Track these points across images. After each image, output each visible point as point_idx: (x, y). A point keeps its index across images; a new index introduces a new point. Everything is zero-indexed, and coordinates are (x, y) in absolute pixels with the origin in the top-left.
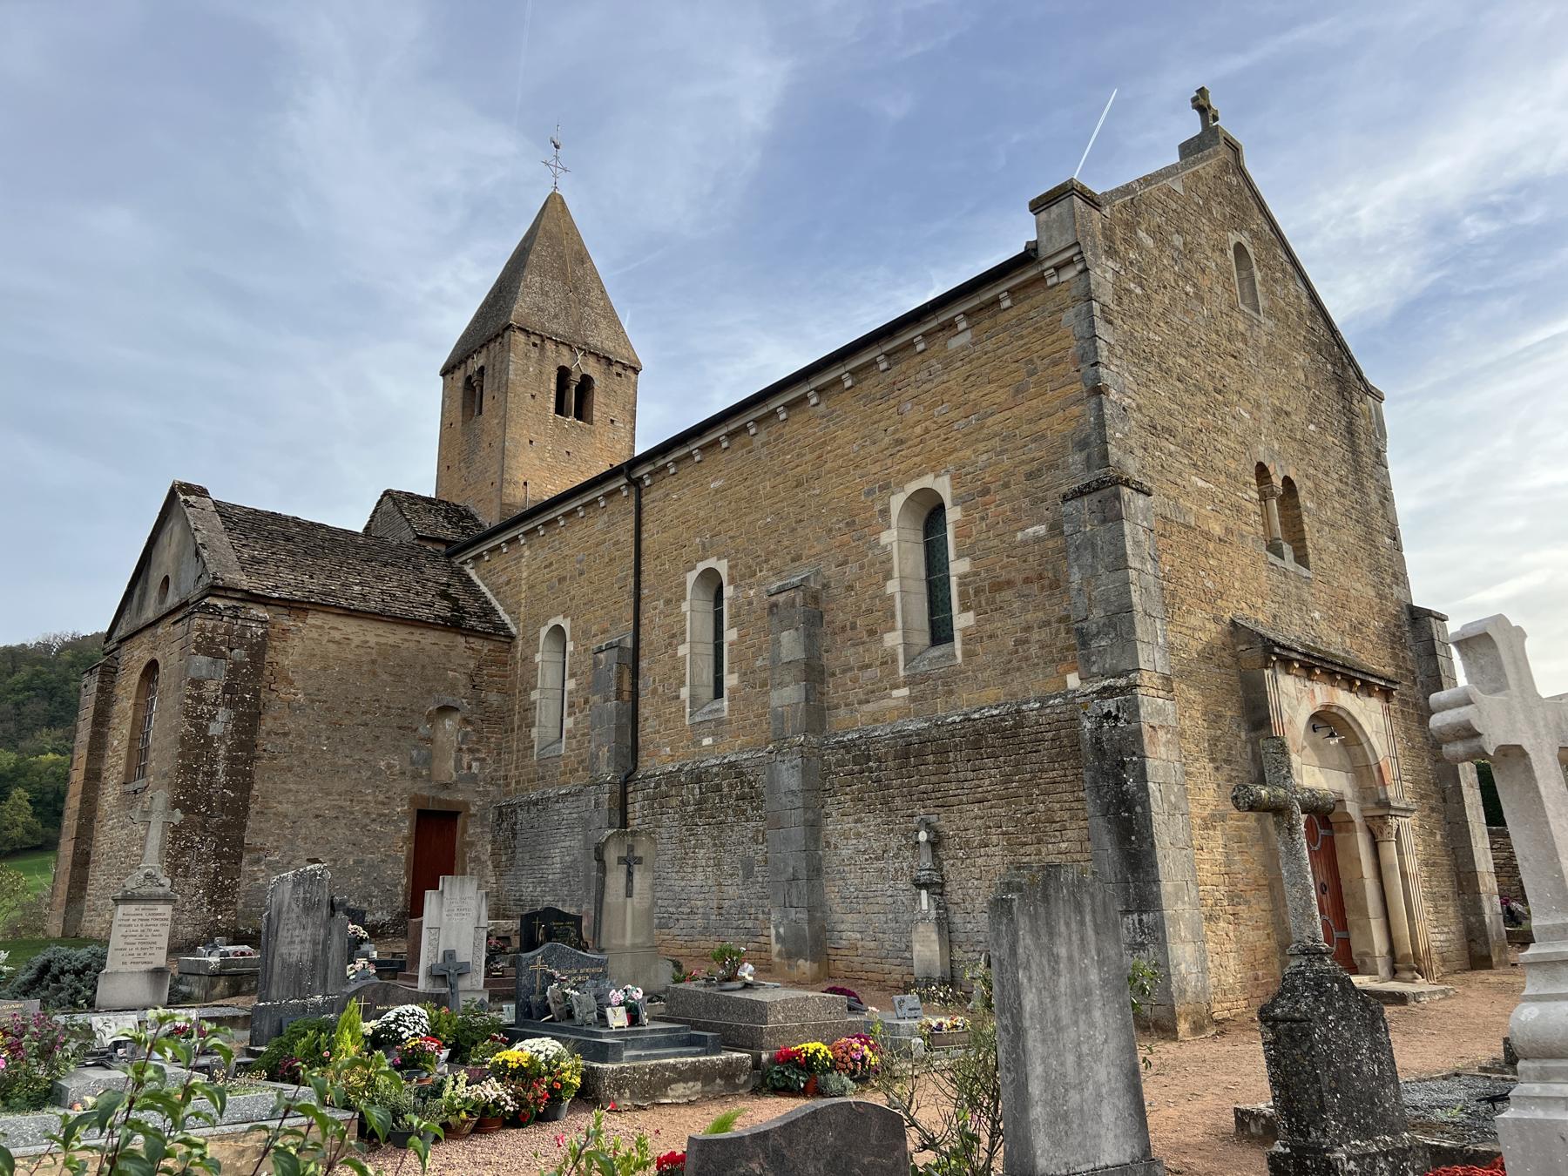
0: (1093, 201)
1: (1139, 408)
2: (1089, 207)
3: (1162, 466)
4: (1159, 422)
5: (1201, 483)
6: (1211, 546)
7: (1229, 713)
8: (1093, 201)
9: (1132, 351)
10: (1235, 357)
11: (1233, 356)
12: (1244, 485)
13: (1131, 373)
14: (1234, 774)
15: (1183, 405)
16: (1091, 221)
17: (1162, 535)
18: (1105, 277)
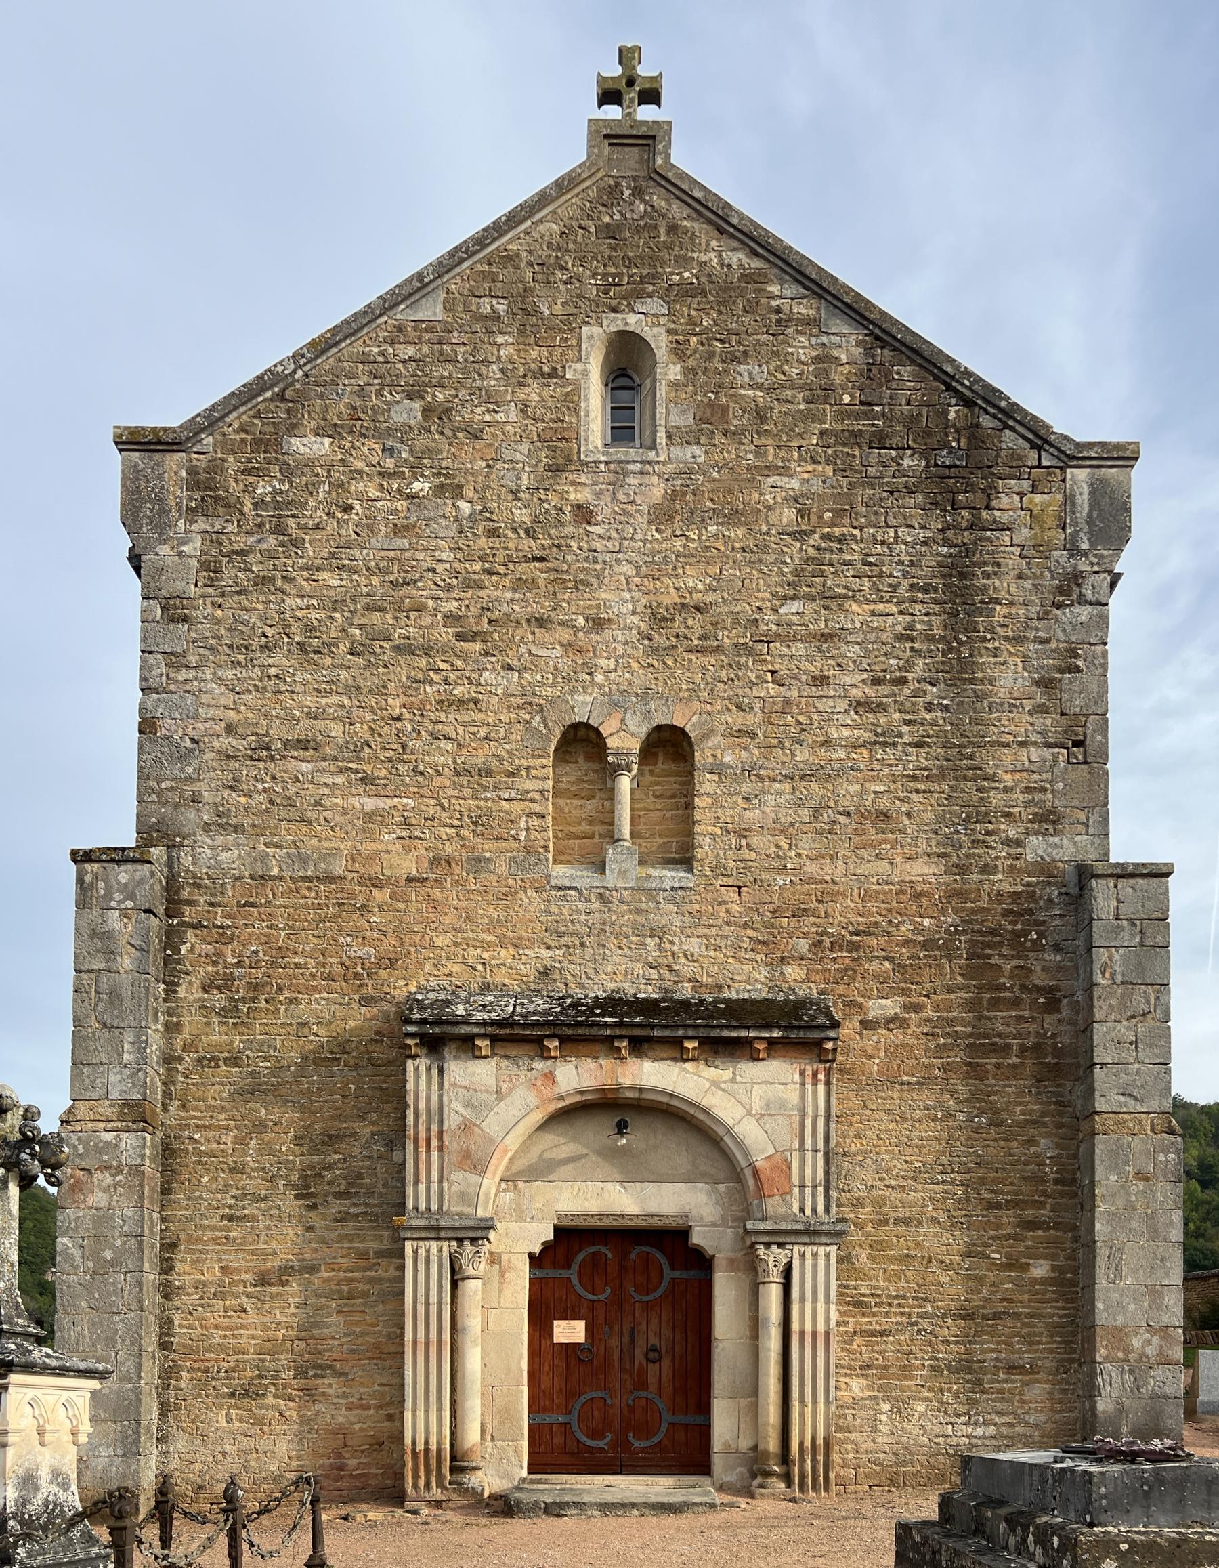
0: (159, 443)
1: (230, 729)
2: (157, 456)
3: (272, 802)
4: (278, 733)
5: (370, 803)
6: (380, 895)
7: (369, 1129)
8: (159, 443)
9: (230, 647)
10: (541, 559)
11: (535, 559)
12: (510, 774)
13: (219, 680)
14: (355, 1210)
15: (353, 690)
16: (160, 477)
17: (244, 905)
18: (180, 555)
